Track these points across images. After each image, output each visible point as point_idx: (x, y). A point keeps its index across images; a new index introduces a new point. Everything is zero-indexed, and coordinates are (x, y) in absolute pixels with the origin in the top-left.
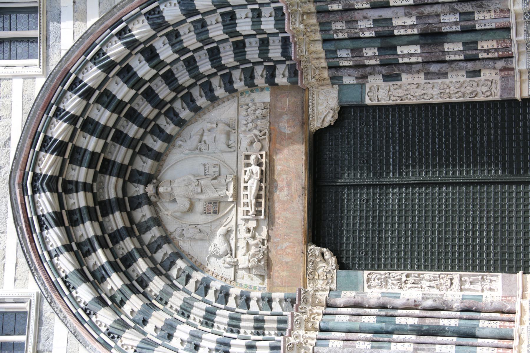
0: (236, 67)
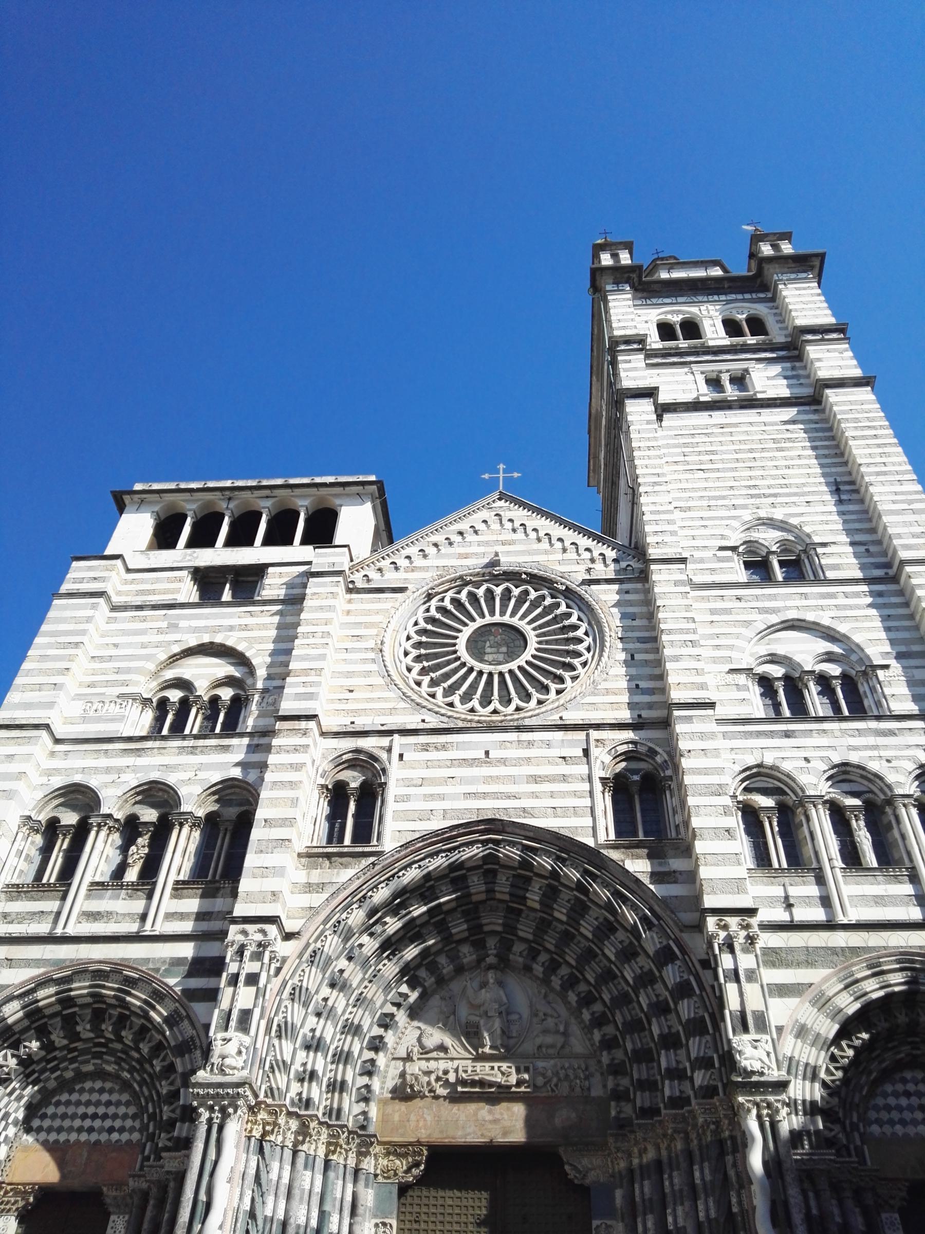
0: (626, 1053)
